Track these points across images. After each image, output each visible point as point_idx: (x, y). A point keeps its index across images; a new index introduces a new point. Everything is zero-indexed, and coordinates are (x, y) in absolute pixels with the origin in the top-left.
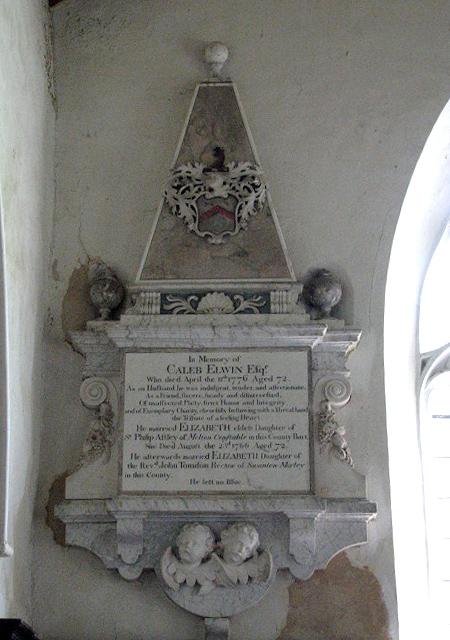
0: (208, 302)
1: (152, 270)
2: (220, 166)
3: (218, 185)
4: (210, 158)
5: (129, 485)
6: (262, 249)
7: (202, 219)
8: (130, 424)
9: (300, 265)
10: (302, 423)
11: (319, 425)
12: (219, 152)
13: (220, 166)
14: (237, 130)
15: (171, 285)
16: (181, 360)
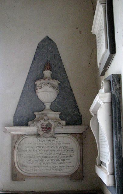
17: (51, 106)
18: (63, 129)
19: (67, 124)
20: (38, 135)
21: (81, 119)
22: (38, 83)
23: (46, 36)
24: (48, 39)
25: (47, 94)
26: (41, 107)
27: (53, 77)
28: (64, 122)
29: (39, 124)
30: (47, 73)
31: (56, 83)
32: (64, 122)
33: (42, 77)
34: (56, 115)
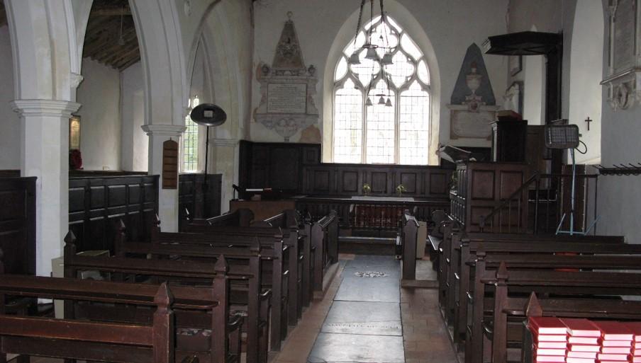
0: (286, 73)
1: (274, 65)
2: (289, 42)
3: (288, 47)
4: (287, 40)
5: (269, 111)
6: (298, 62)
7: (285, 54)
8: (269, 99)
9: (307, 65)
10: (304, 99)
11: (309, 99)
12: (289, 39)
13: (289, 42)
14: (293, 34)
15: (279, 69)
16: (280, 85)
17: (475, 93)
18: (483, 108)
19: (487, 105)
20: (469, 111)
21: (495, 102)
22: (468, 76)
23: (472, 43)
24: (474, 46)
25: (473, 84)
26: (468, 93)
27: (478, 73)
28: (484, 103)
29: (470, 104)
30: (474, 70)
31: (480, 76)
32: (484, 103)
33: (470, 73)
34: (480, 98)
